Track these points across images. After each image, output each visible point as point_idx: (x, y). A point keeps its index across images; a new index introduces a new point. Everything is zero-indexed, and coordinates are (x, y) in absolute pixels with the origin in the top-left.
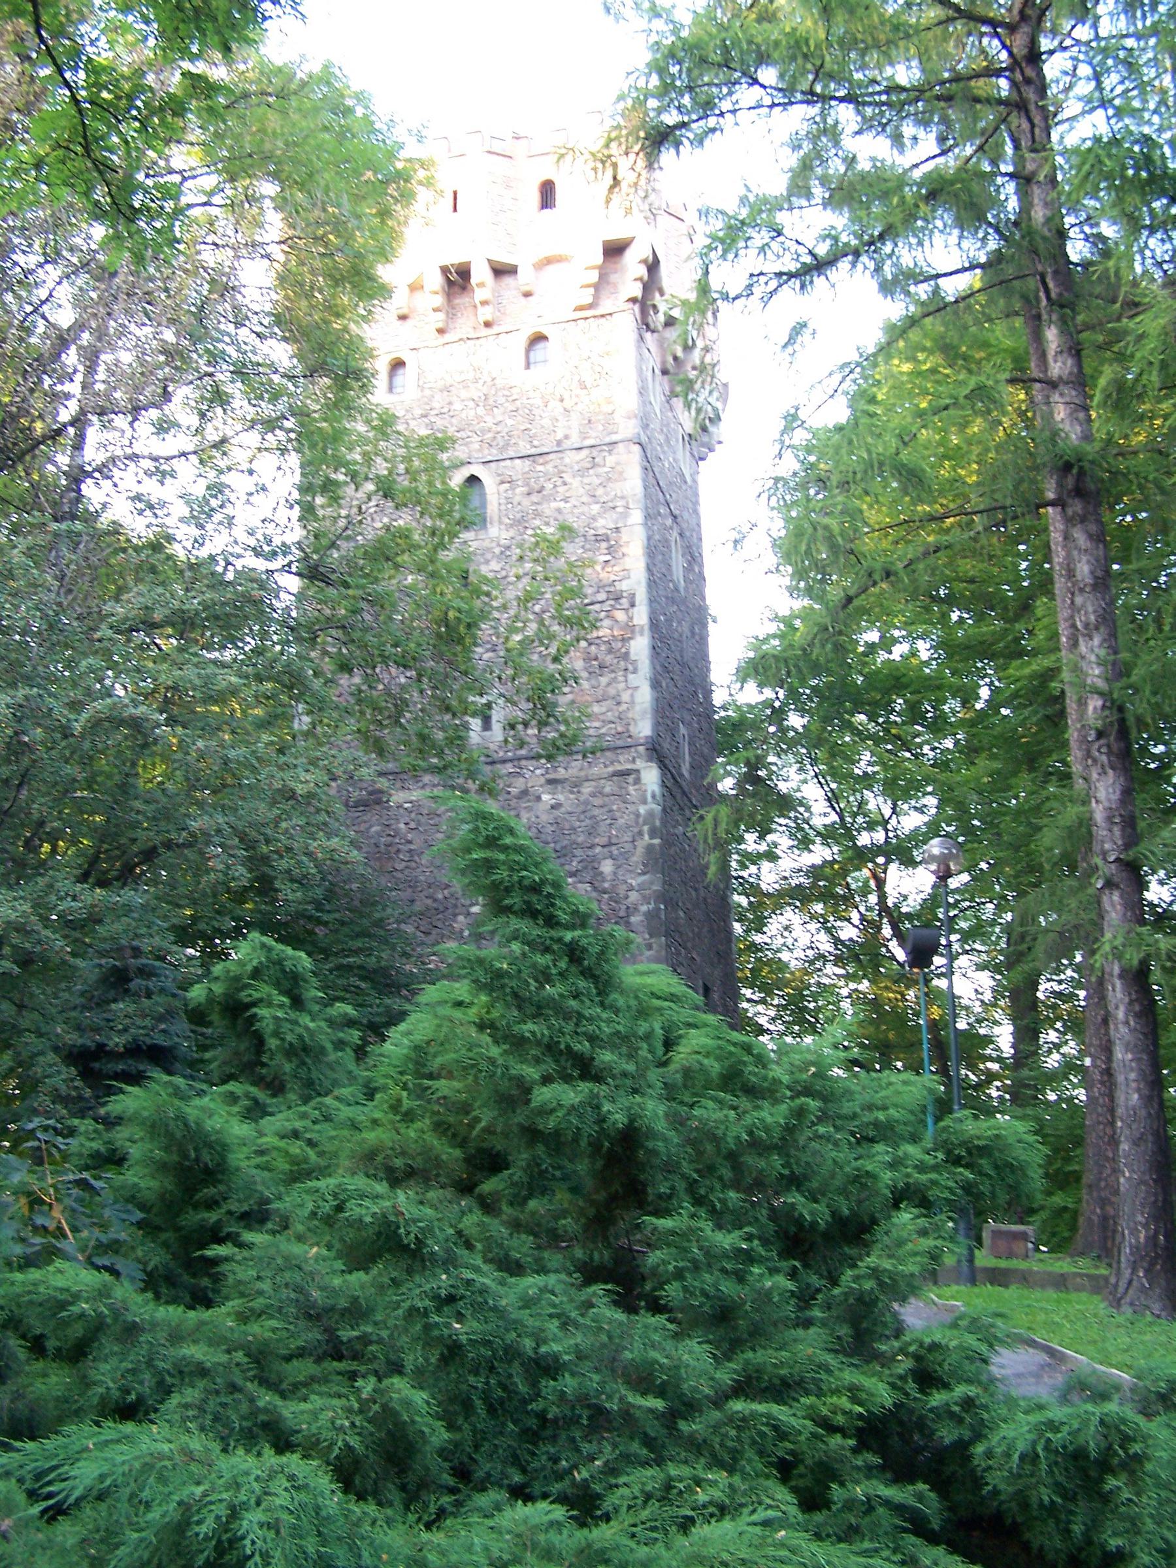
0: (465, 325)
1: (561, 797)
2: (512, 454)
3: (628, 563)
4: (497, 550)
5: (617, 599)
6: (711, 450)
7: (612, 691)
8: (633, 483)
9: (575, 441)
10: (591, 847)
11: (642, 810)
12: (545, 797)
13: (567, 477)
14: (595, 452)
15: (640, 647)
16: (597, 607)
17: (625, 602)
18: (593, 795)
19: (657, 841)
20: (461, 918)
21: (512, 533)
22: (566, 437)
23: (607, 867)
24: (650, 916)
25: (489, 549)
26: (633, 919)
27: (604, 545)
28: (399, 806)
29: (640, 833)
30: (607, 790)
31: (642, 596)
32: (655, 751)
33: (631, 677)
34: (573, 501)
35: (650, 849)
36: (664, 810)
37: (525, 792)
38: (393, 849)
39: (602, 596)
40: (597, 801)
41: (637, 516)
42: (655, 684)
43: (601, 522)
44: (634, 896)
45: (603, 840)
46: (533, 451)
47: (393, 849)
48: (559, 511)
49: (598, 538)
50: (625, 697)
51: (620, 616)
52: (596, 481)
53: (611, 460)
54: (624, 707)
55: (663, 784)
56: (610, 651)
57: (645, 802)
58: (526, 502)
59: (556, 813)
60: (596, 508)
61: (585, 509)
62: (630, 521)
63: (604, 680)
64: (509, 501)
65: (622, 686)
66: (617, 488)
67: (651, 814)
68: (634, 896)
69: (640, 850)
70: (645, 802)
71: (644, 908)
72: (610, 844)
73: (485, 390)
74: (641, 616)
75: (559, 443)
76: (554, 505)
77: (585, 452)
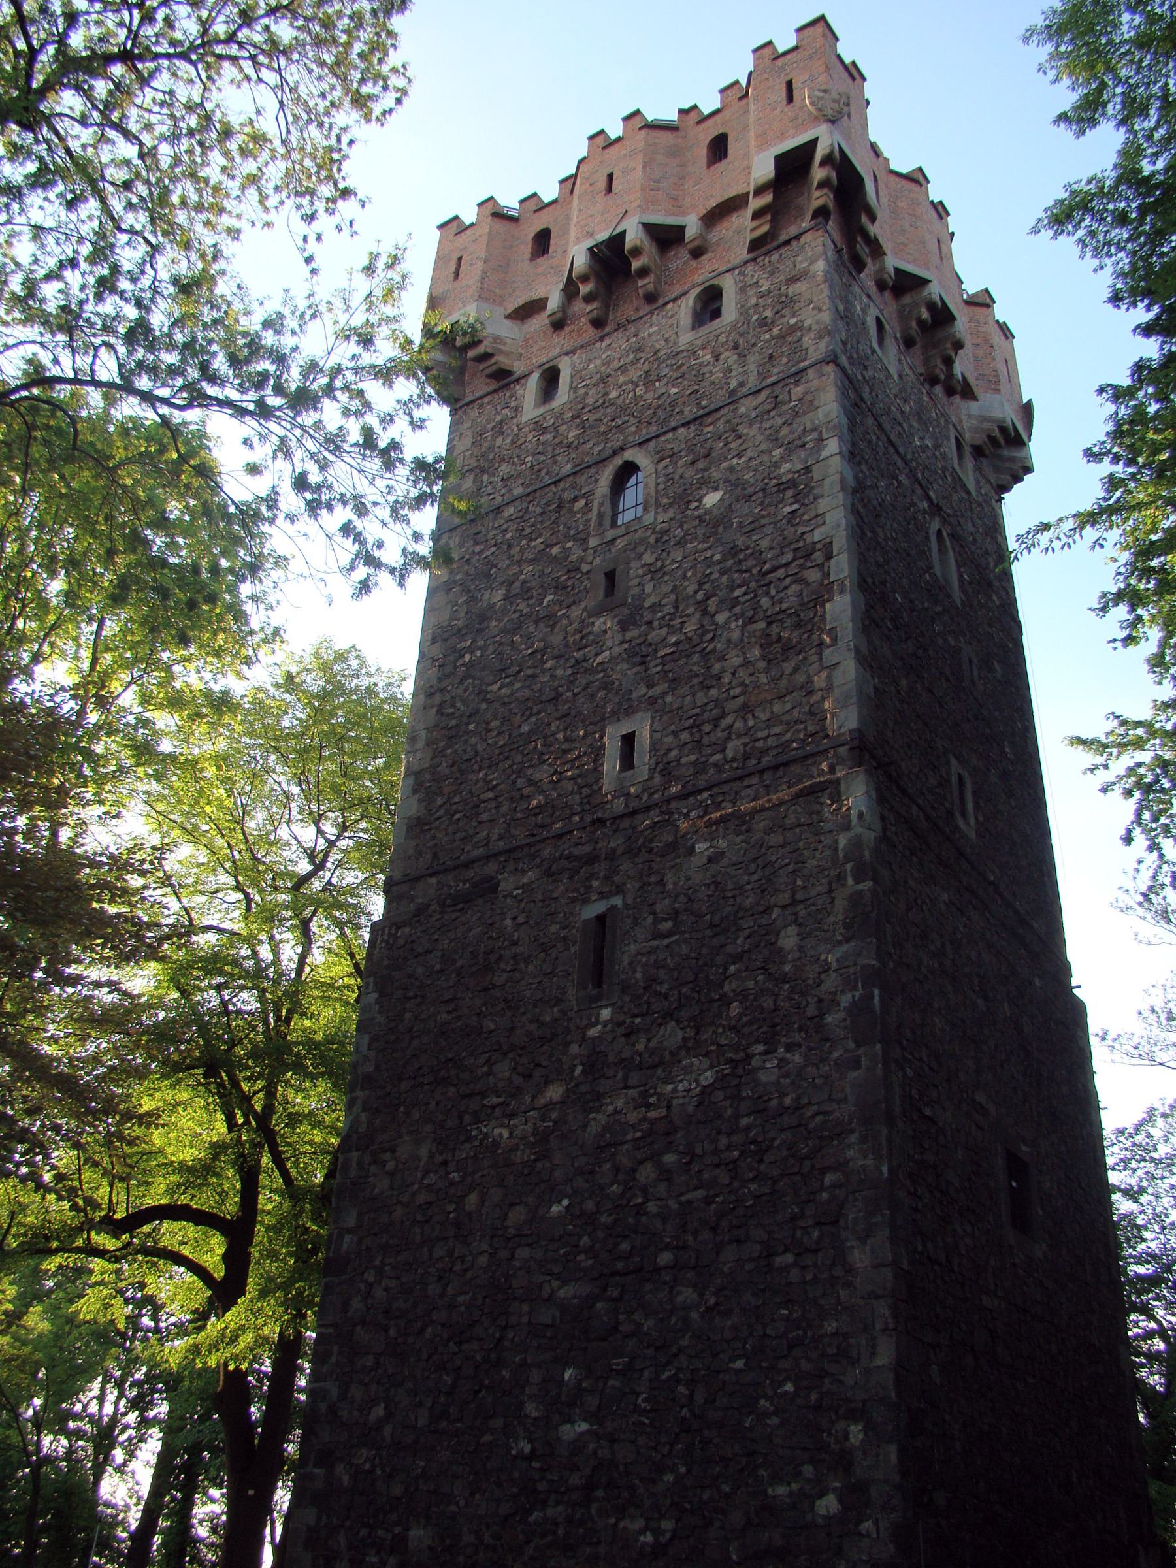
0: (628, 309)
1: (722, 843)
2: (673, 424)
3: (822, 505)
4: (652, 540)
5: (808, 556)
6: (1018, 479)
7: (800, 678)
8: (828, 402)
9: (752, 382)
10: (768, 910)
11: (842, 842)
12: (700, 847)
13: (742, 429)
14: (777, 390)
15: (841, 609)
16: (781, 573)
17: (818, 557)
18: (770, 831)
19: (866, 885)
20: (574, 1049)
21: (670, 514)
22: (742, 384)
23: (789, 939)
24: (860, 1009)
25: (643, 541)
26: (829, 1019)
27: (790, 493)
28: (510, 895)
29: (840, 878)
30: (791, 820)
31: (840, 541)
32: (864, 749)
33: (827, 652)
34: (750, 453)
35: (855, 900)
36: (884, 838)
37: (673, 846)
38: (493, 957)
39: (789, 557)
40: (775, 839)
41: (832, 446)
42: (867, 660)
43: (787, 466)
44: (831, 981)
45: (784, 898)
46: (701, 412)
47: (493, 957)
48: (731, 469)
49: (782, 487)
50: (819, 681)
51: (813, 576)
52: (779, 421)
53: (797, 391)
54: (816, 697)
55: (881, 800)
56: (798, 625)
57: (847, 827)
58: (689, 473)
59: (715, 868)
60: (777, 453)
61: (765, 458)
62: (824, 454)
63: (788, 667)
64: (668, 477)
65: (816, 666)
66: (807, 421)
67: (857, 843)
68: (831, 981)
69: (840, 904)
70: (847, 827)
71: (845, 1000)
72: (794, 903)
73: (646, 367)
74: (842, 566)
75: (732, 393)
76: (725, 464)
77: (764, 395)
